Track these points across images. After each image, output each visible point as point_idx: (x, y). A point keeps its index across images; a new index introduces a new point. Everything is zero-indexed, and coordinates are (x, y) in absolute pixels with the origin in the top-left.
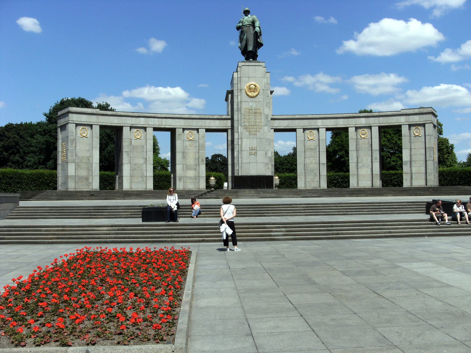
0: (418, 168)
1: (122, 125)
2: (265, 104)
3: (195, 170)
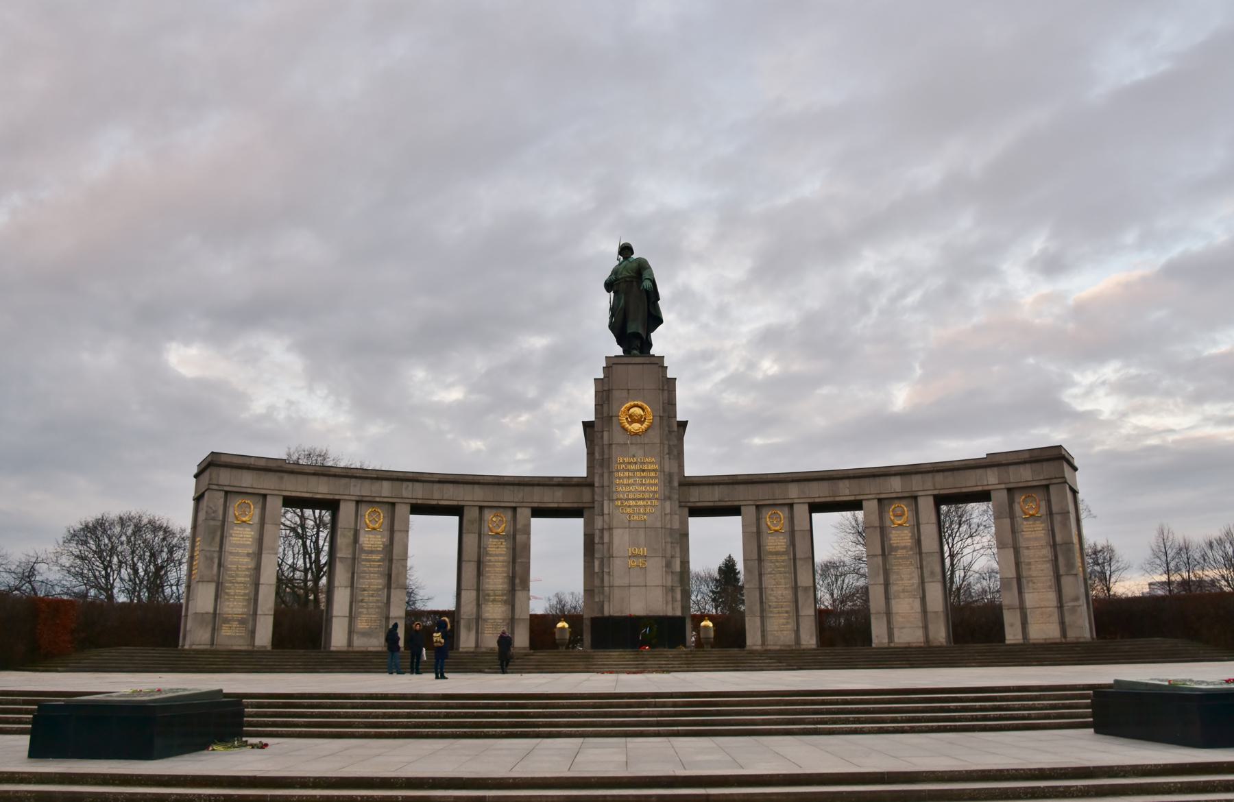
1: (337, 497)
2: (666, 450)
3: (505, 602)
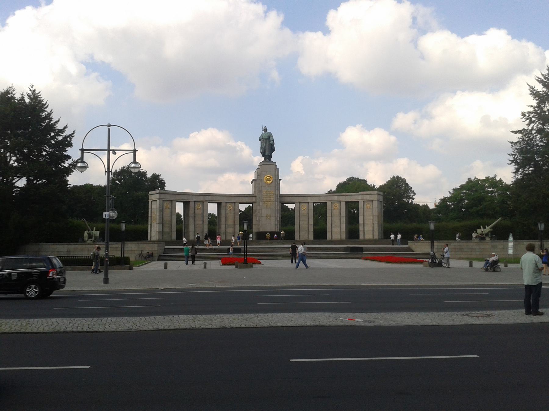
0: (369, 228)
